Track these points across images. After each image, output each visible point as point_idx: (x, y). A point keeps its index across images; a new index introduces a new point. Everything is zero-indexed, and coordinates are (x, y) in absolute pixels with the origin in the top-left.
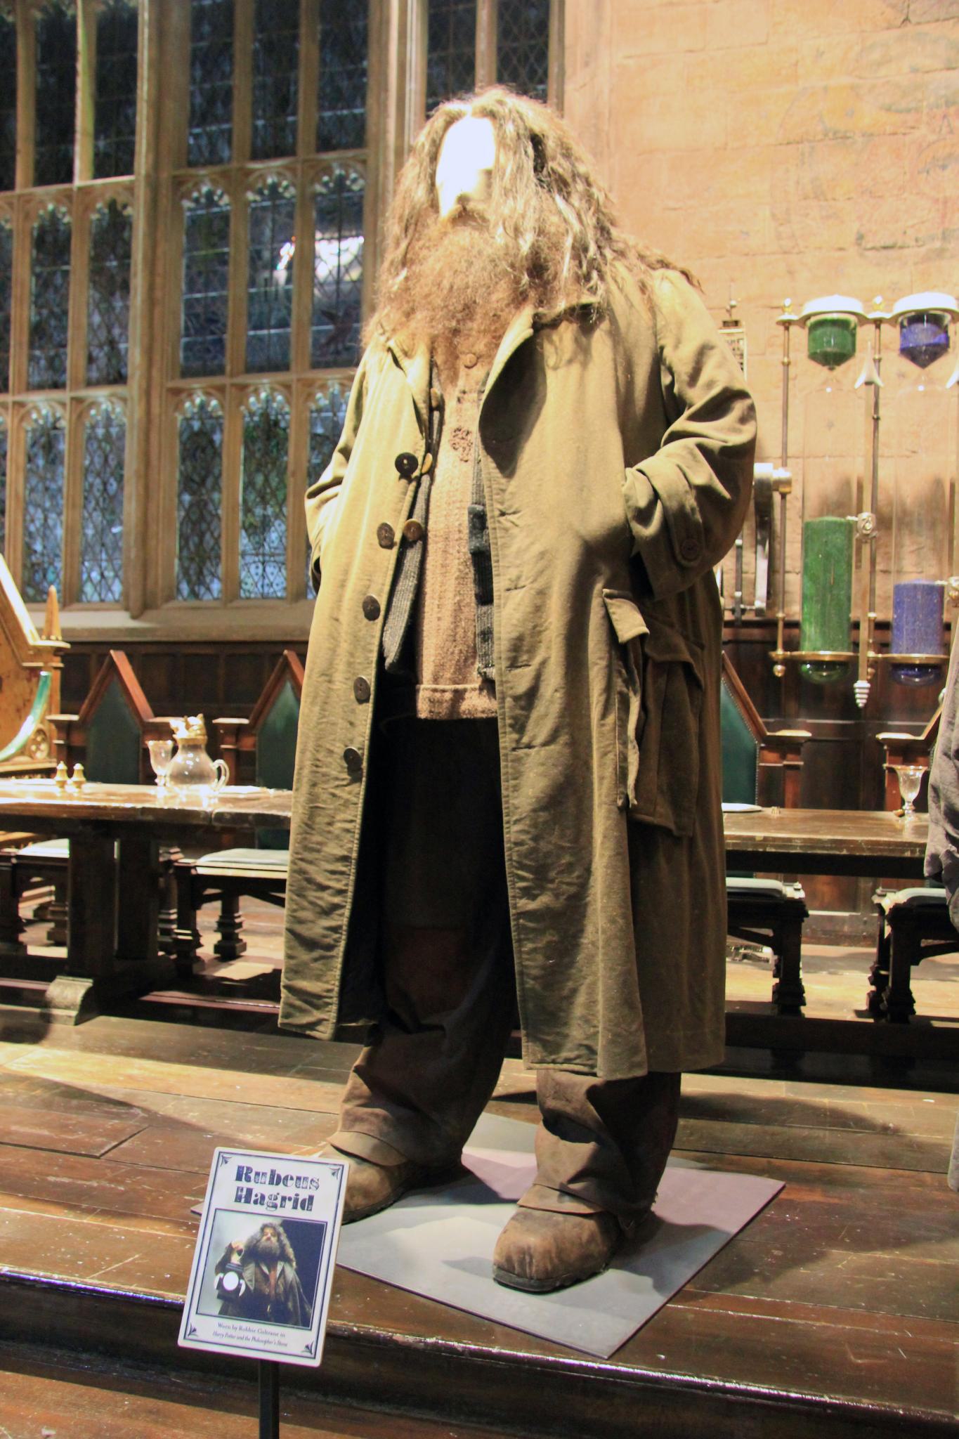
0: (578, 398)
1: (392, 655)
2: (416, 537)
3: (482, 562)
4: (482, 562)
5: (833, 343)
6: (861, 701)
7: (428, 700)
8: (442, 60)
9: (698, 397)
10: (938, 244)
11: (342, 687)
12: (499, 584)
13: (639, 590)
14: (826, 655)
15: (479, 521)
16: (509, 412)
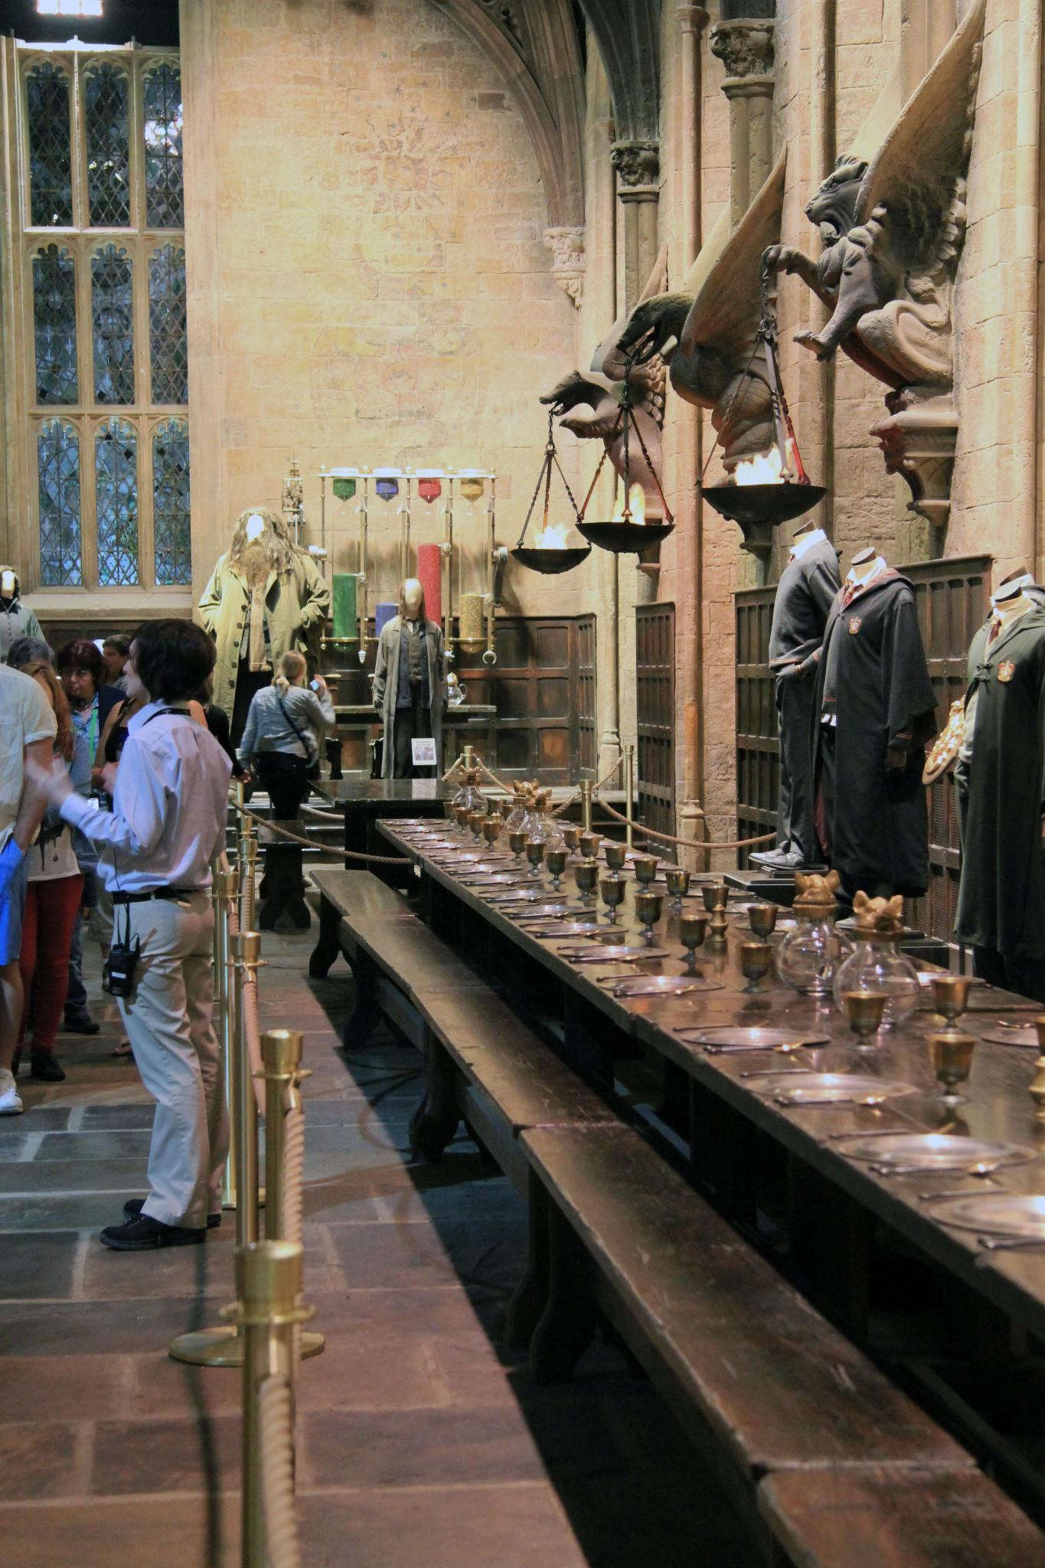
0: (288, 594)
1: (244, 656)
2: (248, 626)
3: (266, 634)
4: (266, 634)
5: (346, 488)
6: (362, 660)
7: (253, 666)
8: (43, 159)
9: (317, 592)
10: (397, 418)
11: (227, 663)
12: (272, 638)
13: (305, 640)
14: (345, 639)
15: (265, 623)
16: (272, 598)
